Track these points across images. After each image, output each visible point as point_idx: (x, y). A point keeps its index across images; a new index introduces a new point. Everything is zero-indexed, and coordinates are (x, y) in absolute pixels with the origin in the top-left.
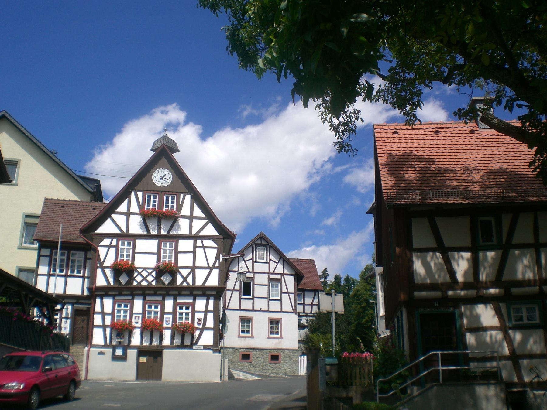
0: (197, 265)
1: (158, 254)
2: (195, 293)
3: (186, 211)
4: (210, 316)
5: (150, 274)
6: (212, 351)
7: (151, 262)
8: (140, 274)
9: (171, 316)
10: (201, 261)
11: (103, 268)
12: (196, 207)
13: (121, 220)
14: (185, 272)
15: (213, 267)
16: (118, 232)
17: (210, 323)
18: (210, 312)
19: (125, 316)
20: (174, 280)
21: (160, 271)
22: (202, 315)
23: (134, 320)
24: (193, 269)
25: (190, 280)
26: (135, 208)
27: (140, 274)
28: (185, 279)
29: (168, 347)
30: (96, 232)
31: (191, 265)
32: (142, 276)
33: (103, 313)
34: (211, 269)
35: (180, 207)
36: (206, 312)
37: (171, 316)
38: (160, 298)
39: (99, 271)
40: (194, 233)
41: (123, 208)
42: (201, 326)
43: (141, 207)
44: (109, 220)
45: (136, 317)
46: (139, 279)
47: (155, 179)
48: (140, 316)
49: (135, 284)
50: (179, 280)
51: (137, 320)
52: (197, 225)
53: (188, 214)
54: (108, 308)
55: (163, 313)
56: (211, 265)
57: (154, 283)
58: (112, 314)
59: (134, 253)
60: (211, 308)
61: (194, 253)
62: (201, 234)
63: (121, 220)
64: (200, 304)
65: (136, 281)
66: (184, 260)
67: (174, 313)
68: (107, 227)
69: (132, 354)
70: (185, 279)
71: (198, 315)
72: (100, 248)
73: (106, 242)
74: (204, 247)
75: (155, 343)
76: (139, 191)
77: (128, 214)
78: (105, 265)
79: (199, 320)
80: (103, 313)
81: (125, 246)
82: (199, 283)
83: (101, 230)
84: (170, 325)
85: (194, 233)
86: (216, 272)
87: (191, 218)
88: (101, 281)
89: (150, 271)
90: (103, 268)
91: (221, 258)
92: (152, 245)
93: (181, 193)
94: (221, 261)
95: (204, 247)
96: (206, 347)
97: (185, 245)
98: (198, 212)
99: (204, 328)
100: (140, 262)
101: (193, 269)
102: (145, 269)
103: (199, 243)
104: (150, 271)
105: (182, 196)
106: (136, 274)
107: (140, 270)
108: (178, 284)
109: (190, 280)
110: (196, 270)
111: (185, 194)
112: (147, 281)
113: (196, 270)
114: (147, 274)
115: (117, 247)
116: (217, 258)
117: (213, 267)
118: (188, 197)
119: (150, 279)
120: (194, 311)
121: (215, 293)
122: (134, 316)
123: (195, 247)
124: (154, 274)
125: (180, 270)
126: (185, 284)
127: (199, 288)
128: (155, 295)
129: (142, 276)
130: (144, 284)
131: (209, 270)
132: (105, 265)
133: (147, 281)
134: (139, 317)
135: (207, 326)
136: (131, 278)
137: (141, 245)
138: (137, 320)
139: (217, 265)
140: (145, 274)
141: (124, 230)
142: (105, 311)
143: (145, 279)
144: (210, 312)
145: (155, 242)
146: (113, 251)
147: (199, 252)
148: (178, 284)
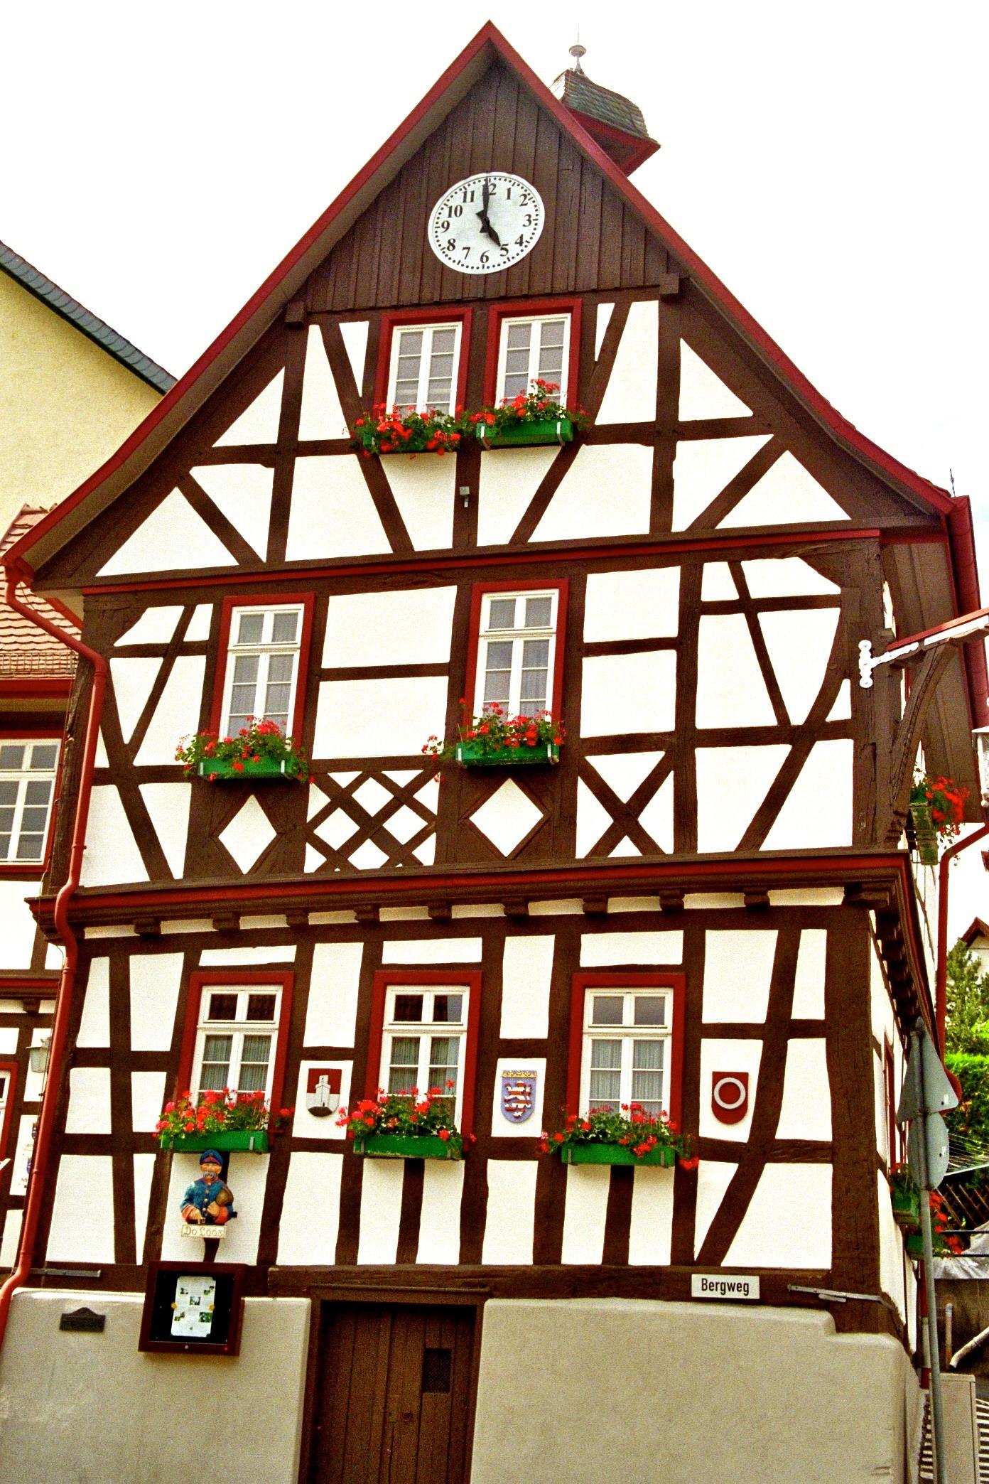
0: (705, 719)
1: (459, 670)
2: (694, 902)
3: (629, 396)
4: (807, 1062)
5: (403, 797)
6: (824, 1317)
7: (409, 720)
8: (342, 800)
9: (538, 1066)
10: (730, 696)
11: (129, 778)
12: (695, 371)
13: (241, 492)
14: (623, 774)
15: (818, 727)
16: (222, 557)
17: (807, 1110)
18: (807, 1029)
19: (251, 1072)
20: (560, 821)
21: (469, 771)
22: (745, 1057)
23: (303, 1101)
24: (680, 747)
25: (658, 820)
26: (323, 415)
27: (342, 800)
28: (625, 816)
29: (513, 1283)
30: (102, 573)
31: (665, 722)
32: (355, 812)
33: (121, 1060)
34: (800, 739)
35: (590, 374)
36: (778, 1030)
37: (538, 1066)
38: (468, 950)
39: (106, 803)
40: (682, 520)
41: (257, 422)
42: (740, 1133)
43: (361, 402)
44: (176, 499)
45: (314, 1075)
46: (337, 830)
47: (444, 238)
48: (346, 1067)
49: (313, 861)
50: (592, 822)
51: (323, 1093)
52: (702, 471)
53: (646, 412)
54: (152, 1030)
55: (488, 1045)
56: (798, 715)
57: (426, 854)
58: (174, 1063)
59: (313, 674)
60: (809, 1001)
61: (685, 645)
62: (735, 520)
63: (241, 492)
64: (737, 971)
65: (322, 847)
66: (624, 697)
67: (561, 1046)
68: (168, 539)
69: (282, 1324)
70: (625, 816)
71: (718, 1056)
72: (116, 664)
73: (157, 624)
74: (749, 607)
75: (439, 1245)
76: (354, 314)
77: (282, 455)
78: (143, 759)
79: (729, 1093)
80: (121, 1060)
81: (264, 636)
82: (719, 834)
83: (134, 557)
84: (533, 1128)
85: (682, 520)
86: (832, 763)
87: (664, 433)
88: (111, 860)
89: (402, 778)
90: (129, 778)
91: (867, 663)
92: (418, 621)
93: (602, 294)
94: (866, 682)
95: (748, 606)
96: (780, 1288)
97: (631, 602)
98: (705, 393)
99: (763, 1149)
100: (354, 724)
101: (680, 747)
102: (373, 768)
103: (717, 581)
104: (402, 778)
105: (605, 312)
106: (317, 800)
107: (343, 779)
108: (584, 847)
109: (658, 820)
110: (700, 753)
111: (624, 295)
112: (385, 841)
113: (700, 753)
114: (387, 797)
115: (214, 650)
116: (842, 665)
117: (818, 727)
118: (644, 318)
119: (404, 825)
120: (691, 1032)
121: (833, 898)
122: (306, 1066)
123: (693, 608)
124: (429, 795)
125: (596, 761)
126: (626, 849)
127: (717, 873)
128: (443, 927)
129: (355, 812)
130: (369, 858)
131: (784, 750)
132: (140, 760)
133: (385, 841)
134: (335, 1077)
135: (785, 1131)
136: (293, 830)
137: (363, 626)
138: (323, 1093)
139: (841, 710)
140: (372, 797)
141: (259, 543)
142: (137, 1044)
143: (371, 827)
144: (807, 1029)
145: (443, 599)
146: (190, 670)
147: (722, 638)
148: (584, 847)
